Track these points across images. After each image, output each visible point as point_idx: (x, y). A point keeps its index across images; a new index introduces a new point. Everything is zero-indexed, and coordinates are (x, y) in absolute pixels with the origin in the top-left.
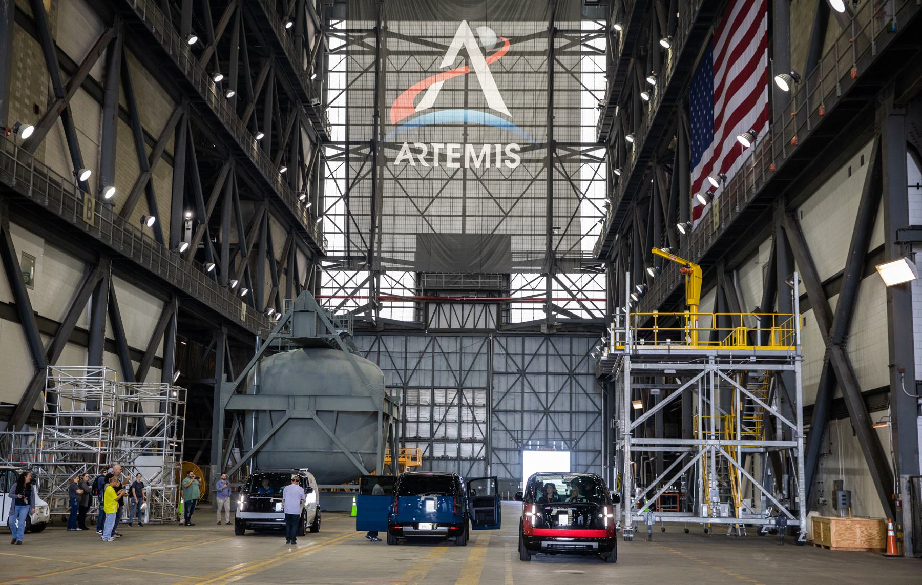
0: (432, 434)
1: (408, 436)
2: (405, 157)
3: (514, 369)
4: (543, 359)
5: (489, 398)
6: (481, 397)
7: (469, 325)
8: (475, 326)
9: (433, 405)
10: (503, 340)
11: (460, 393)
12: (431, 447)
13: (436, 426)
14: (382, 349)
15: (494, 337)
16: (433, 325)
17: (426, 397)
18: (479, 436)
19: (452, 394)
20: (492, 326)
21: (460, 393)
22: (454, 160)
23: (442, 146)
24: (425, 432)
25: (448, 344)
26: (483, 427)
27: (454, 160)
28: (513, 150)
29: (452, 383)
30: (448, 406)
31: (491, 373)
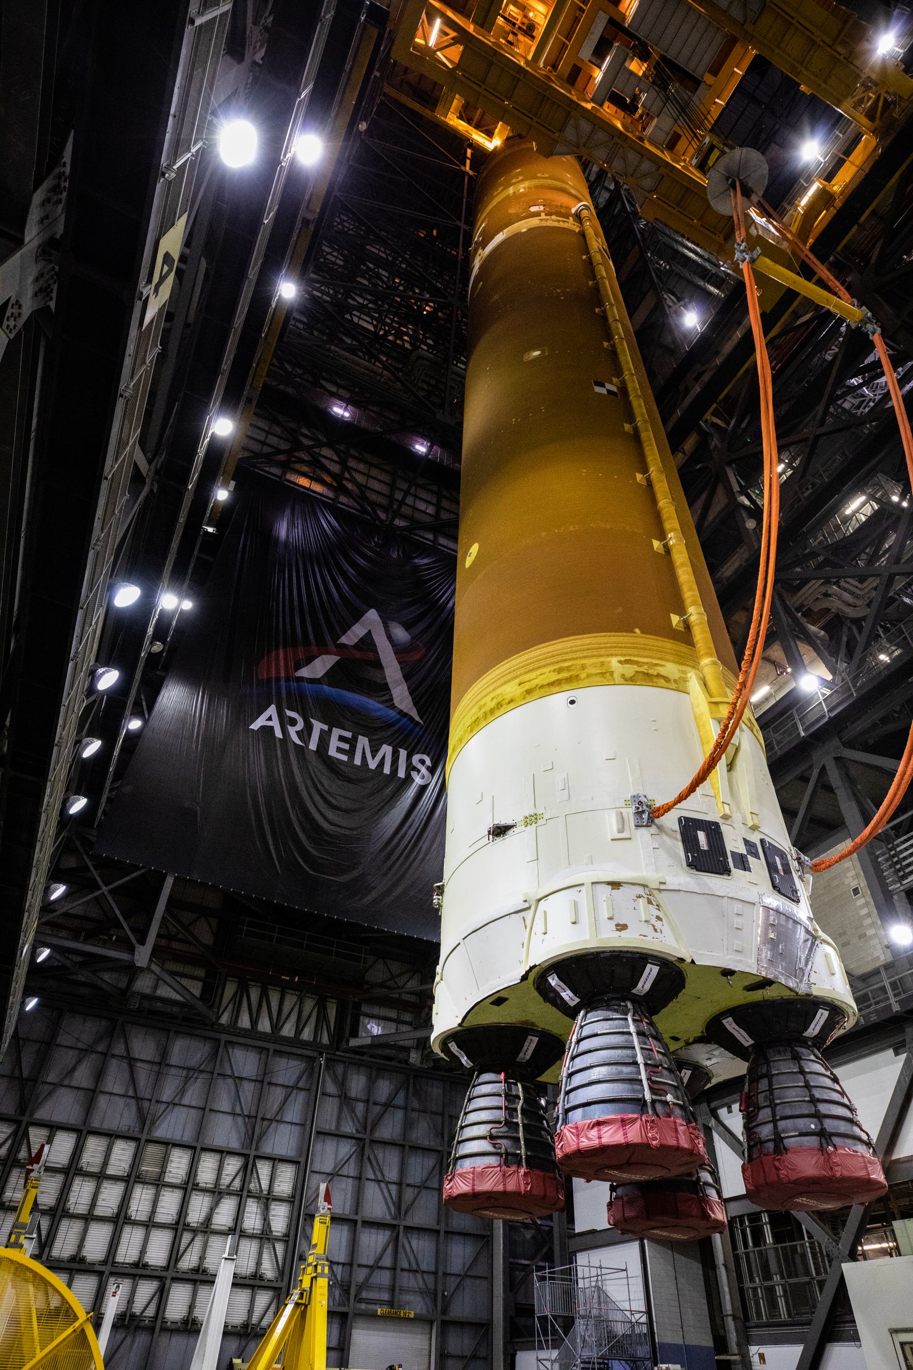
0: (175, 1254)
1: (120, 1258)
2: (269, 723)
3: (349, 1128)
4: (400, 1114)
5: (300, 1184)
6: (285, 1183)
7: (288, 1030)
8: (299, 1031)
9: (189, 1186)
10: (340, 1069)
11: (248, 1170)
12: (162, 1295)
13: (186, 1237)
14: (119, 1049)
15: (328, 1060)
16: (224, 1019)
17: (178, 1164)
18: (268, 1270)
19: (233, 1165)
20: (325, 1040)
21: (248, 1170)
22: (339, 750)
23: (326, 728)
24: (157, 1255)
25: (245, 1062)
26: (280, 1248)
27: (339, 750)
28: (422, 762)
29: (235, 1145)
30: (217, 1193)
31: (311, 1133)
